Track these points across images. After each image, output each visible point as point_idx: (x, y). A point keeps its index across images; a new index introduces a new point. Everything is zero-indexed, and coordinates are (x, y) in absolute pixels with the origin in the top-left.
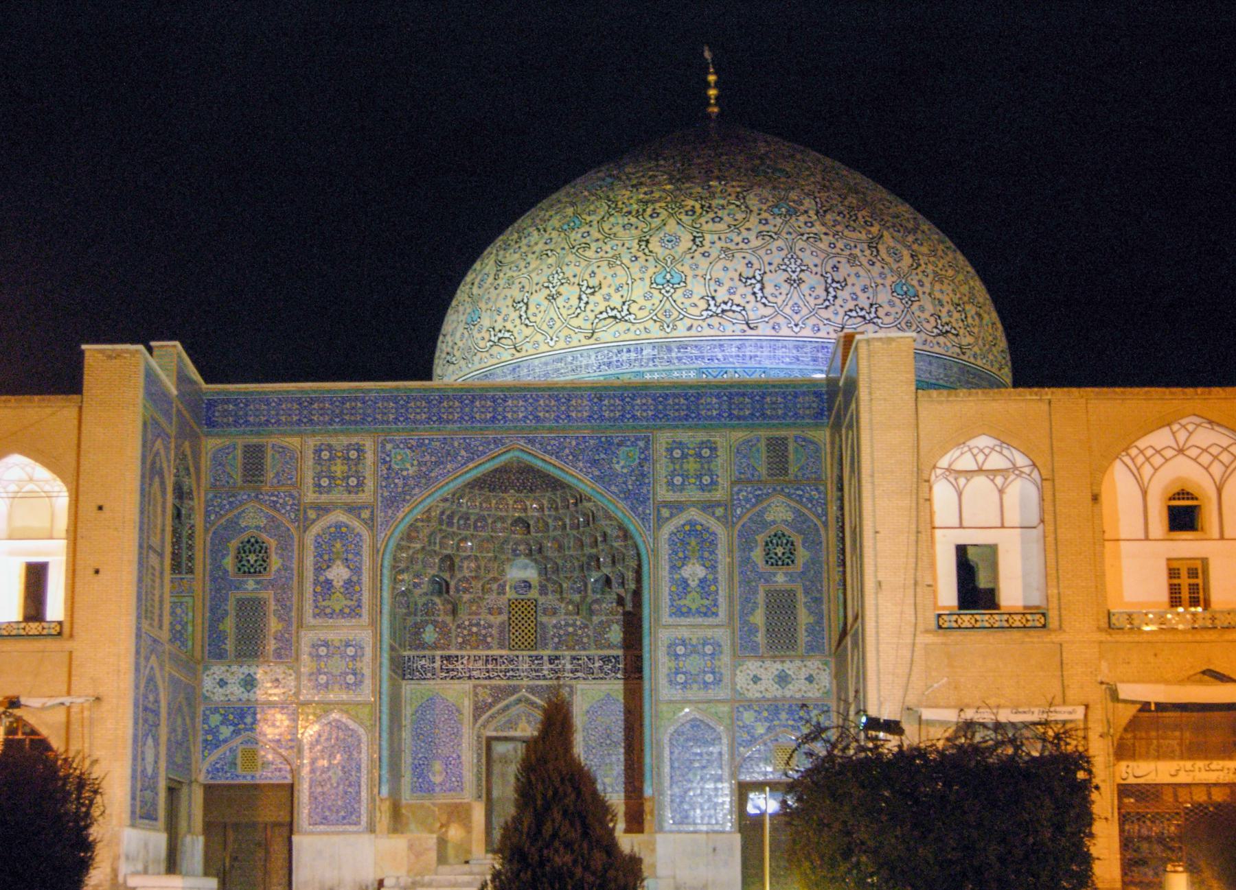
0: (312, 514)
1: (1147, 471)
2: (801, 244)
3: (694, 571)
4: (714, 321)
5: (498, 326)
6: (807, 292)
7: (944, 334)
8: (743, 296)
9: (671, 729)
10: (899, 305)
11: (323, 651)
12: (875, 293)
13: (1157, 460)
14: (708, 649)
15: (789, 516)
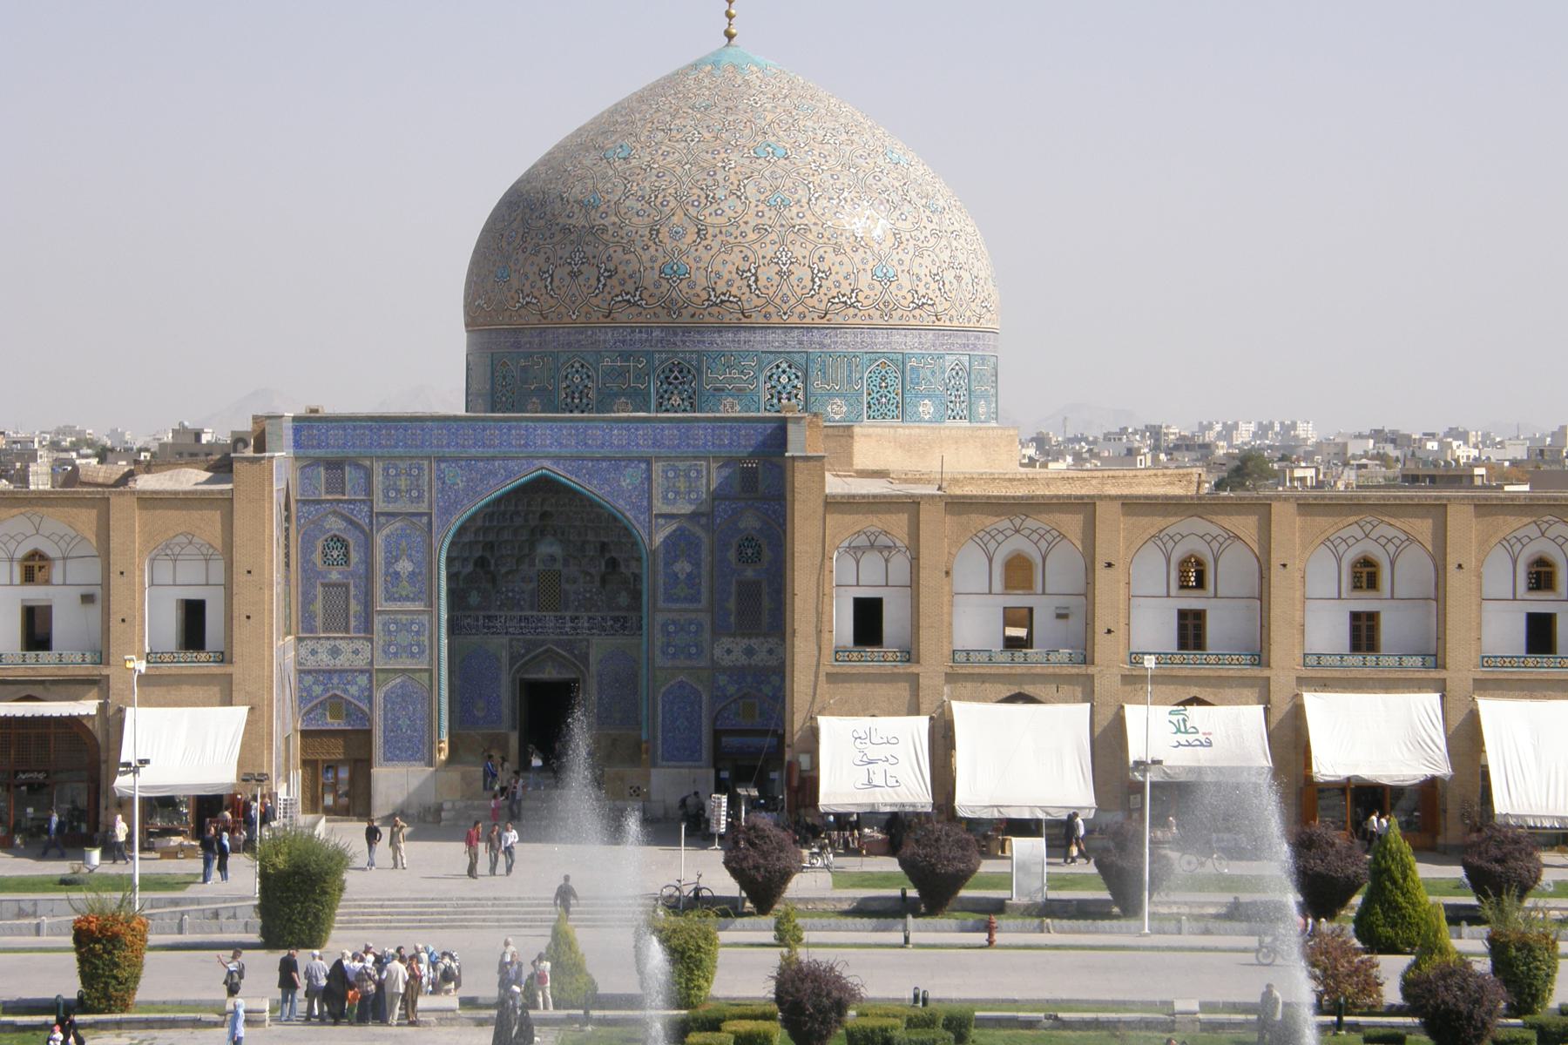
0: (382, 519)
1: (992, 545)
2: (791, 237)
3: (683, 567)
4: (715, 310)
5: (527, 290)
6: (795, 283)
7: (919, 307)
8: (740, 288)
9: (663, 689)
10: (878, 288)
11: (393, 627)
12: (856, 280)
13: (1000, 538)
14: (693, 628)
15: (758, 525)
